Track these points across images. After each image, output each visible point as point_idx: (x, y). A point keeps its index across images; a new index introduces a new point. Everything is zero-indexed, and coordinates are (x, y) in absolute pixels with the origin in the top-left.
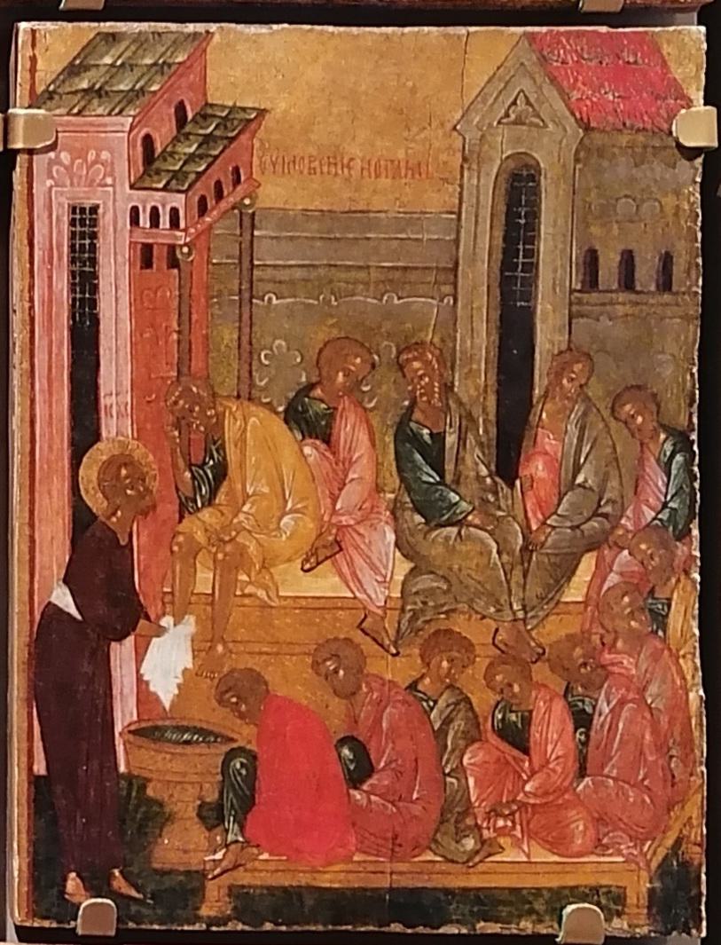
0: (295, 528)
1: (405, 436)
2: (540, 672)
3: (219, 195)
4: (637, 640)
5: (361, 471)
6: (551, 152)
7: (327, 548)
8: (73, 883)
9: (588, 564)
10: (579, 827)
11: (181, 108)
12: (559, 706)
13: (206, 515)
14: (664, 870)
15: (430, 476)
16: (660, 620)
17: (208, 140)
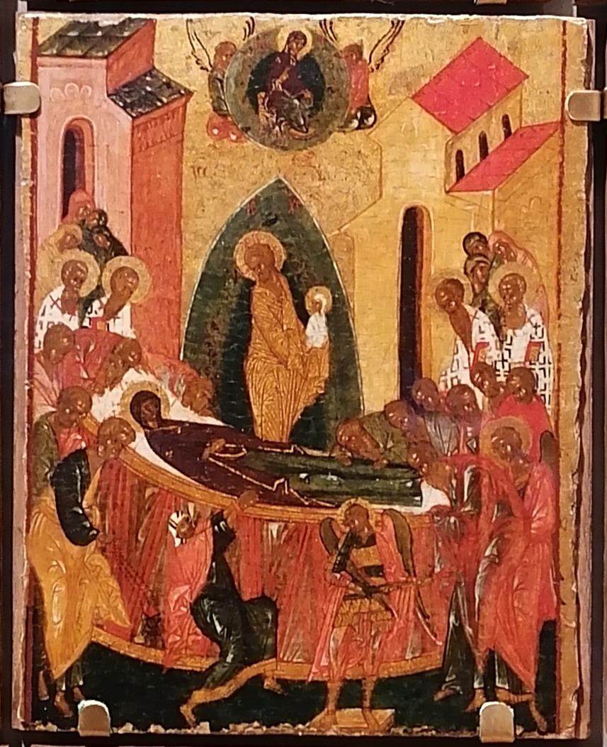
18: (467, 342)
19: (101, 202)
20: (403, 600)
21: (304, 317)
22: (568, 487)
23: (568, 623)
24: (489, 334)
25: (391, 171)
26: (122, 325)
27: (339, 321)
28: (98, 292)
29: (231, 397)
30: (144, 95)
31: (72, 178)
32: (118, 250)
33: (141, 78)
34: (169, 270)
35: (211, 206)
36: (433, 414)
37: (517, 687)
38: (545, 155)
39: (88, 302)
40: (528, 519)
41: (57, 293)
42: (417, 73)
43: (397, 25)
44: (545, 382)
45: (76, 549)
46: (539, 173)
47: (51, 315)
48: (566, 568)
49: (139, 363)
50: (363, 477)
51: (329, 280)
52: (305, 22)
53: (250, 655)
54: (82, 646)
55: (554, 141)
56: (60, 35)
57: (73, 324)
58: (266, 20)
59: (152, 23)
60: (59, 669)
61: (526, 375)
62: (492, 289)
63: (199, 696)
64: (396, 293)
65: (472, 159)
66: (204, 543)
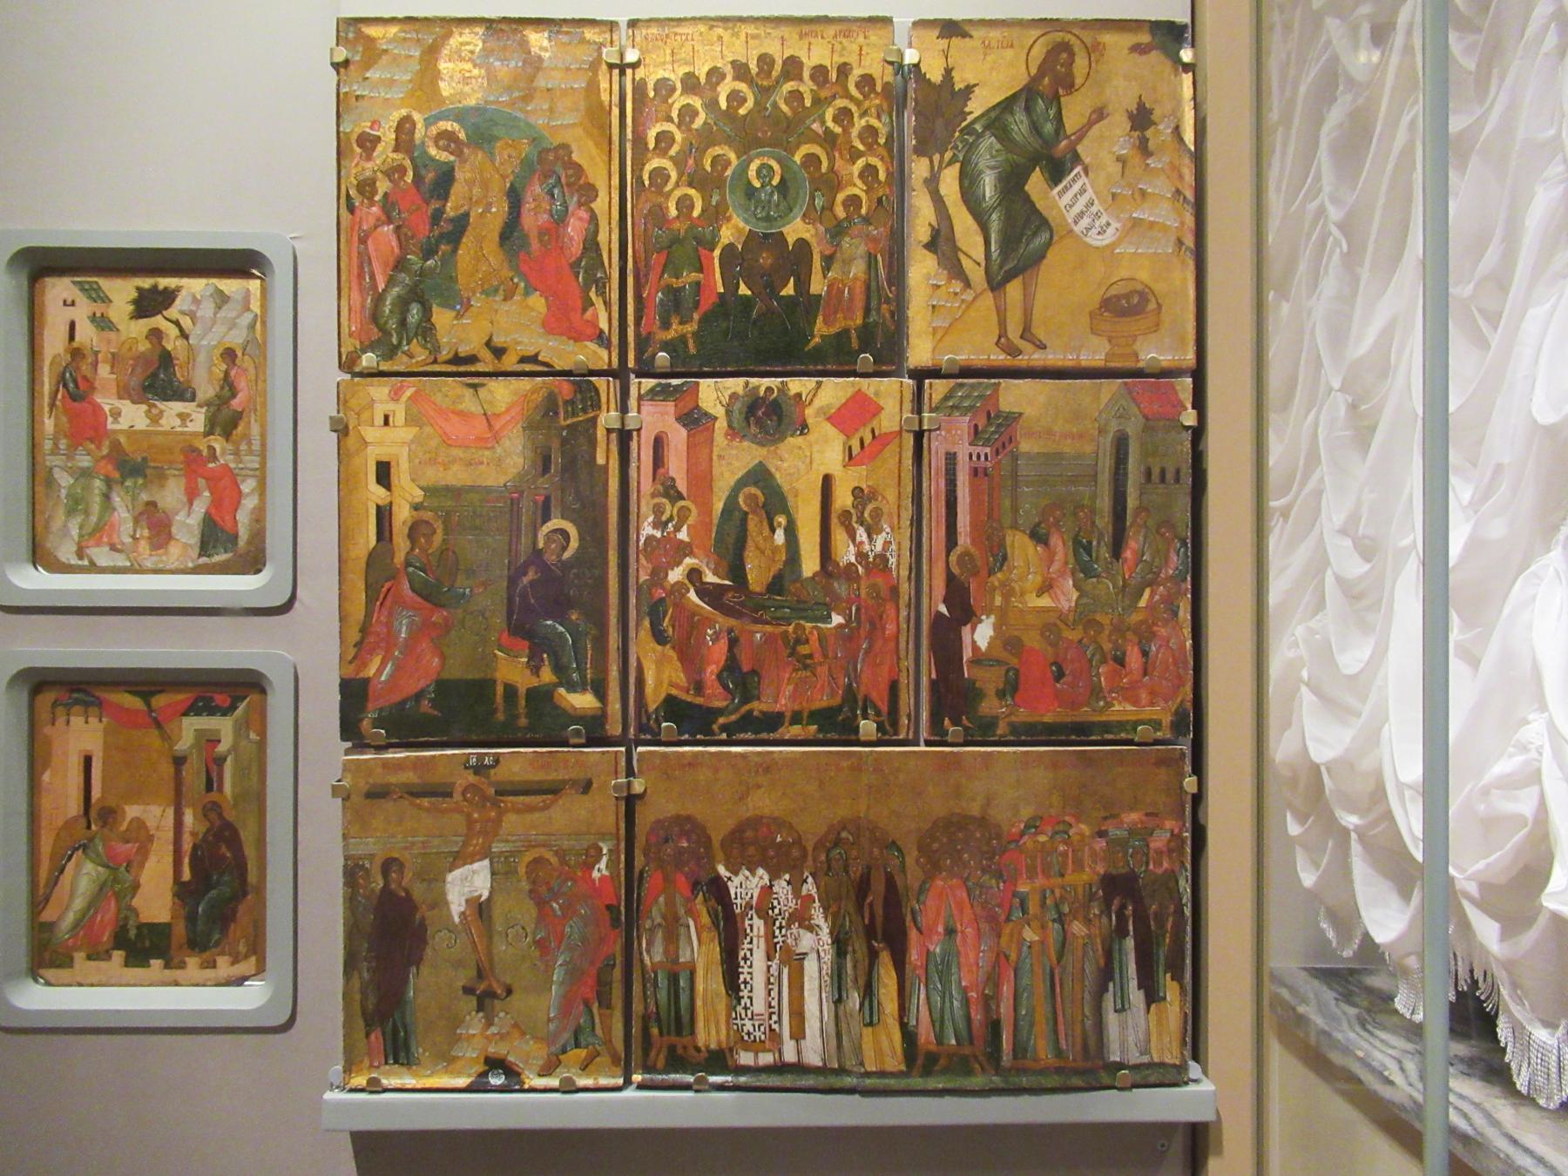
0: (1034, 580)
1: (1077, 542)
2: (1129, 635)
3: (1004, 446)
4: (1166, 622)
5: (1060, 557)
6: (1133, 428)
7: (1046, 588)
8: (947, 722)
9: (1147, 592)
10: (1144, 696)
11: (989, 414)
12: (1136, 649)
13: (999, 575)
14: (1176, 713)
15: (1086, 558)
16: (1175, 614)
17: (999, 426)
18: (854, 540)
19: (672, 473)
20: (822, 671)
21: (773, 531)
22: (903, 613)
23: (903, 681)
24: (865, 538)
25: (816, 456)
26: (683, 535)
27: (791, 531)
28: (671, 519)
29: (737, 571)
30: (694, 419)
31: (658, 461)
32: (681, 497)
33: (692, 411)
34: (706, 508)
35: (727, 475)
36: (838, 578)
37: (878, 713)
38: (893, 448)
39: (666, 523)
40: (884, 629)
41: (651, 519)
42: (829, 406)
43: (819, 384)
44: (893, 561)
45: (659, 648)
46: (889, 455)
47: (648, 530)
48: (902, 654)
49: (691, 554)
50: (802, 609)
51: (785, 511)
52: (773, 382)
53: (746, 700)
54: (663, 696)
55: (897, 441)
56: (652, 390)
57: (658, 534)
58: (754, 381)
59: (697, 384)
60: (652, 707)
61: (882, 558)
62: (866, 515)
63: (721, 720)
64: (818, 518)
65: (856, 450)
66: (723, 644)
